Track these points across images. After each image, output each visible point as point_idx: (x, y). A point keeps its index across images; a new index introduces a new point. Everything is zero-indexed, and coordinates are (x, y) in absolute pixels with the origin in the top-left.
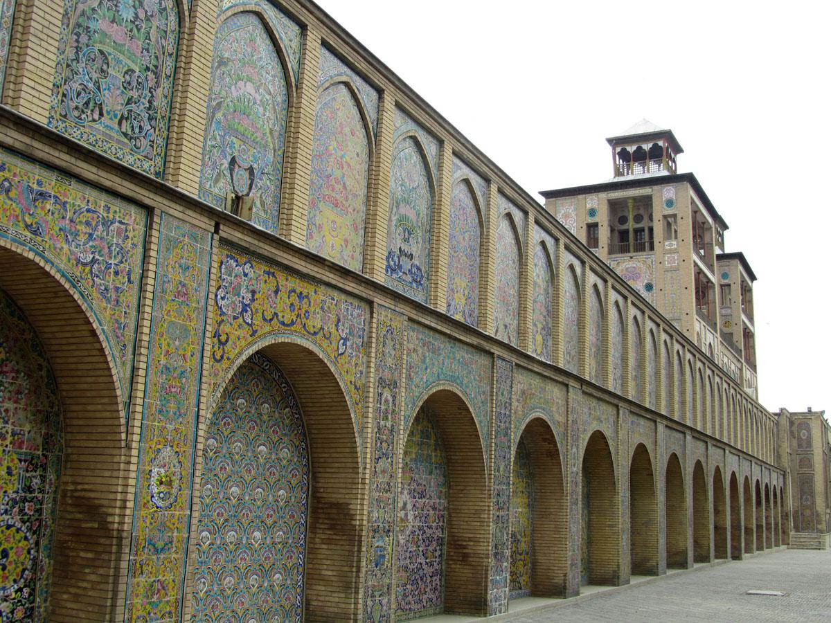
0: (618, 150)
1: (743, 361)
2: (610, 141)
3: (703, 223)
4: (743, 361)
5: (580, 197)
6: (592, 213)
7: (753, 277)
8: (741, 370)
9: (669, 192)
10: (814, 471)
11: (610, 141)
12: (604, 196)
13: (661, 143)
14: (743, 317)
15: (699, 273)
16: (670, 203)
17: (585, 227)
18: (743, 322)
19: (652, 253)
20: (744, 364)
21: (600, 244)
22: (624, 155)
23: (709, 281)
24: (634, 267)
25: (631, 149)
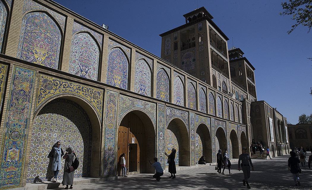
0: (188, 18)
1: (248, 93)
2: (184, 16)
3: (215, 35)
4: (248, 93)
5: (172, 34)
6: (176, 38)
7: (254, 69)
8: (247, 96)
9: (200, 25)
10: (262, 125)
11: (184, 16)
12: (179, 31)
13: (201, 13)
14: (247, 78)
15: (212, 52)
16: (201, 29)
17: (173, 44)
18: (248, 81)
19: (195, 47)
20: (248, 94)
21: (178, 48)
22: (190, 19)
23: (224, 60)
24: (189, 54)
25: (192, 17)
